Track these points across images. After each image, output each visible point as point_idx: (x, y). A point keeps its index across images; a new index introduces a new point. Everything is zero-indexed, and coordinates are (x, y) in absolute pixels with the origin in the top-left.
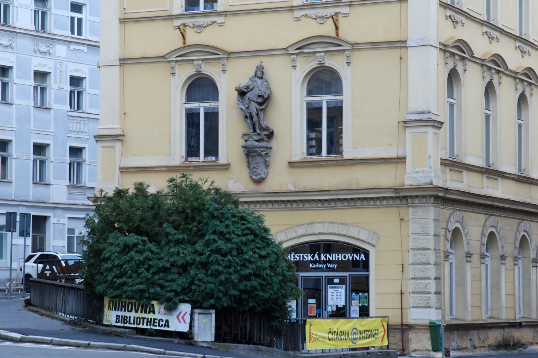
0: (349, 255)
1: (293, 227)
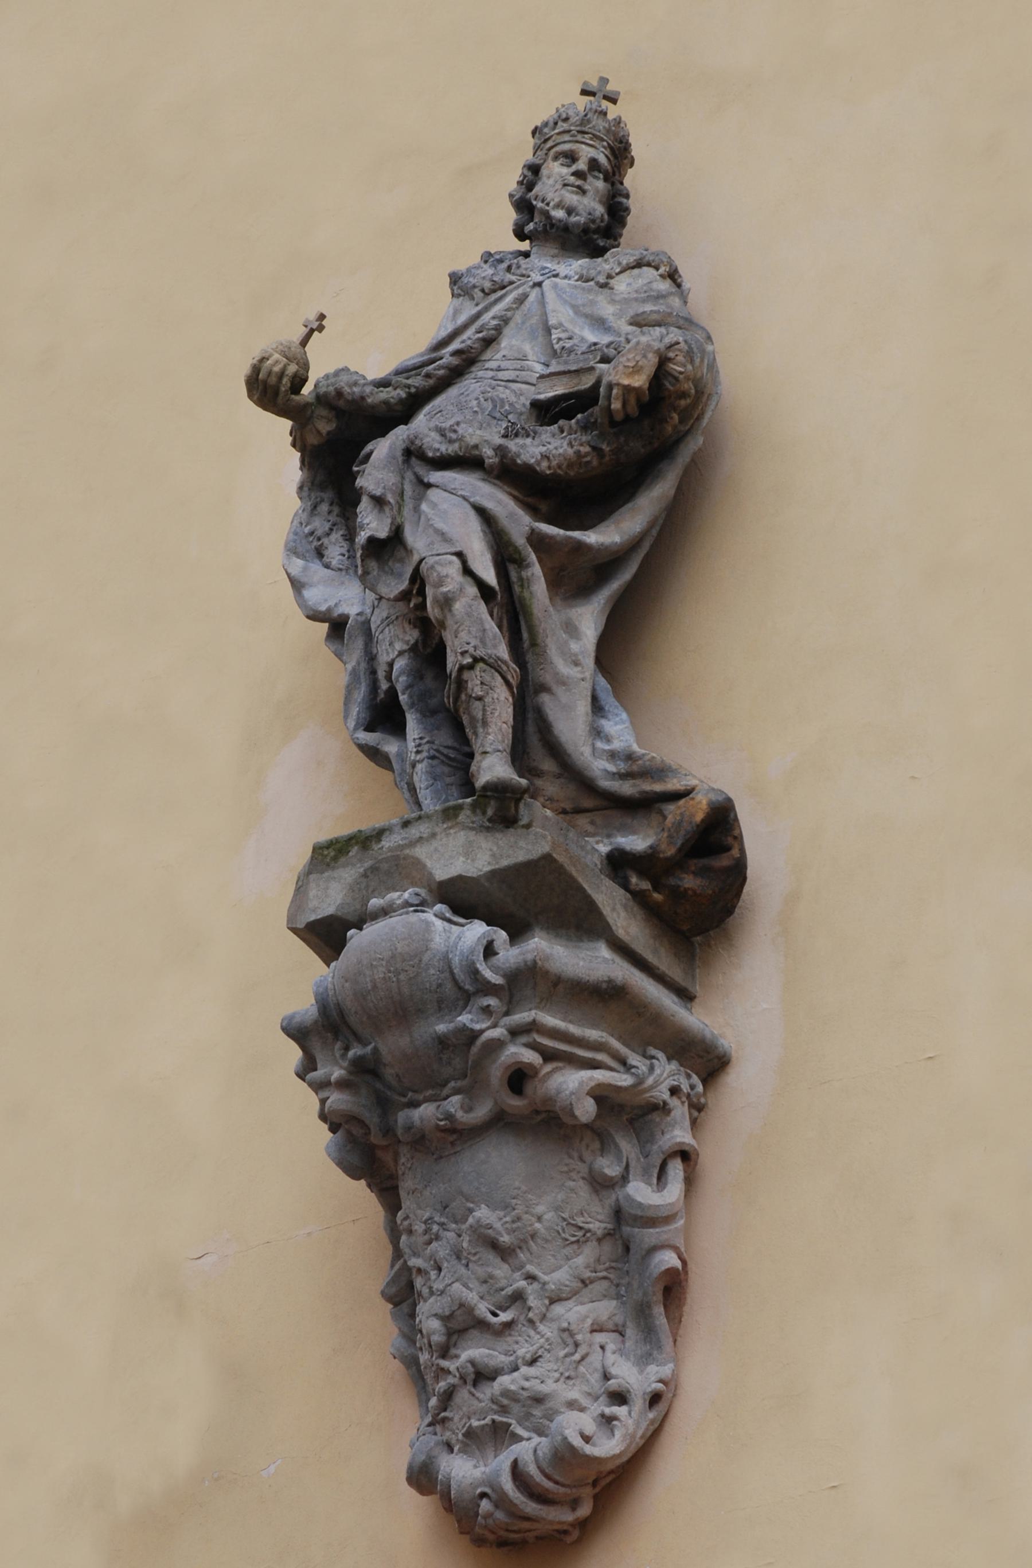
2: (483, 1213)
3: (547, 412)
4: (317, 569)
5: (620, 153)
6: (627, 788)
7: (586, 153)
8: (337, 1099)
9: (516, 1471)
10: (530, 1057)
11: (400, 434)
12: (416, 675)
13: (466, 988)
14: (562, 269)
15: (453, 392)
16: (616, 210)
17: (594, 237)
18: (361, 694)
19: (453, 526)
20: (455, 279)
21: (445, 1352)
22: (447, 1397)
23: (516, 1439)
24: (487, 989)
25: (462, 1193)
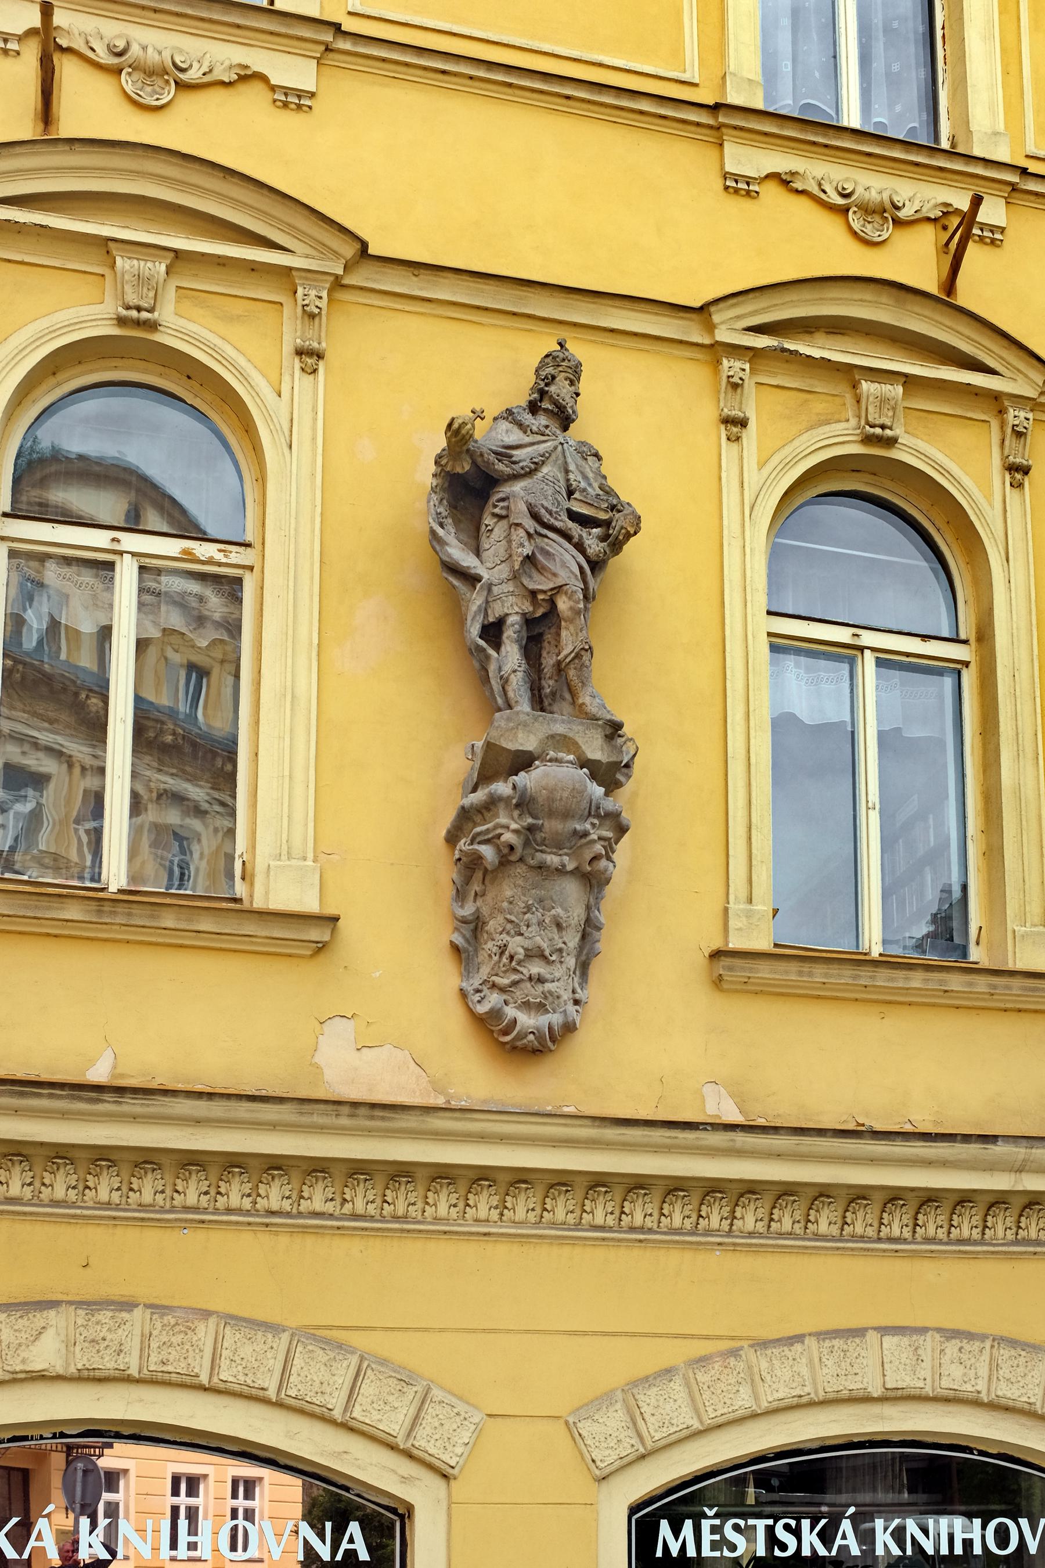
0: (1024, 1522)
1: (734, 1353)
2: (559, 911)
9: (550, 1028)
23: (547, 1012)
25: (552, 899)
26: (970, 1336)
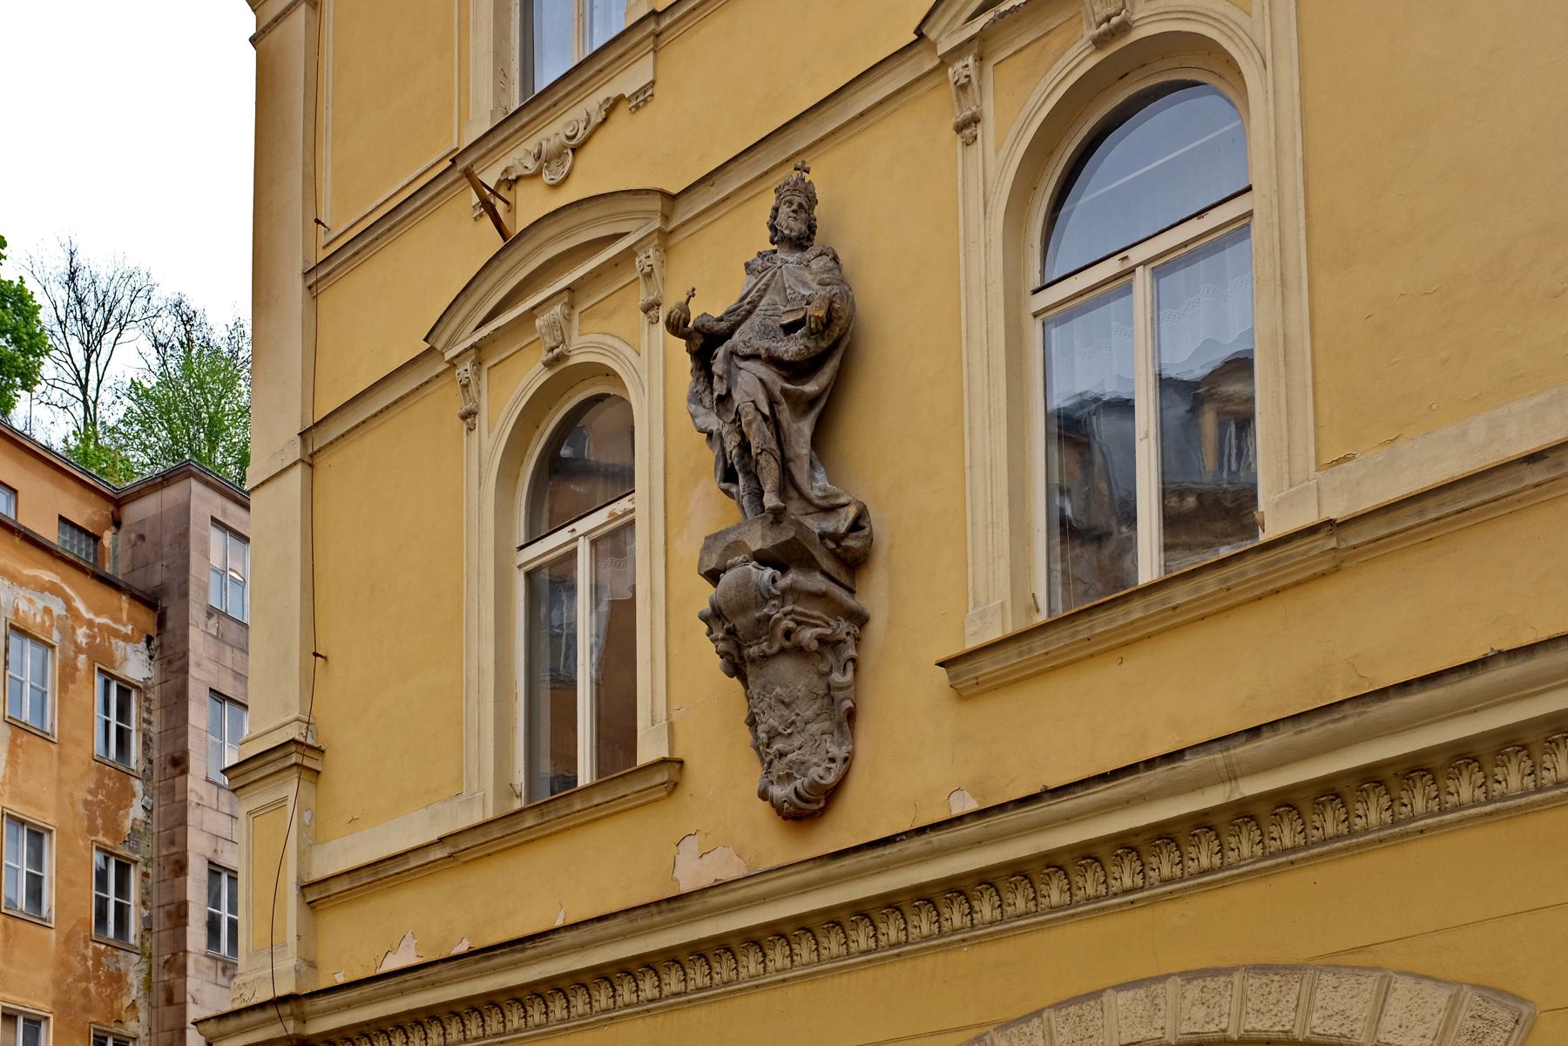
3: (789, 329)
4: (701, 410)
5: (812, 201)
6: (824, 503)
7: (797, 200)
8: (721, 645)
10: (792, 625)
11: (729, 343)
12: (741, 456)
13: (765, 598)
14: (790, 259)
15: (748, 322)
16: (812, 228)
17: (800, 243)
18: (721, 465)
19: (750, 383)
20: (747, 265)
21: (768, 746)
22: (770, 763)
24: (774, 597)
26: (1215, 972)
